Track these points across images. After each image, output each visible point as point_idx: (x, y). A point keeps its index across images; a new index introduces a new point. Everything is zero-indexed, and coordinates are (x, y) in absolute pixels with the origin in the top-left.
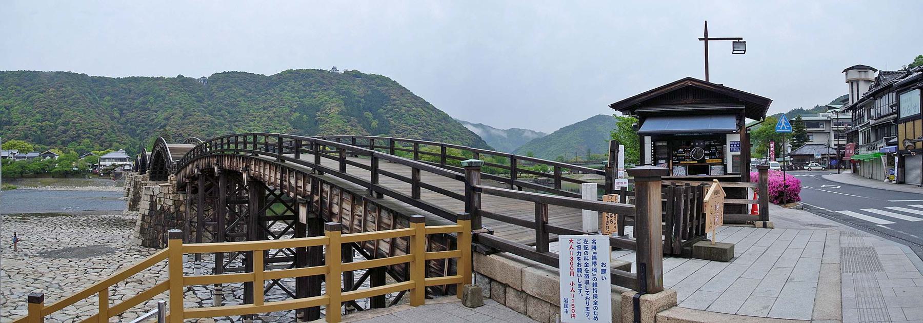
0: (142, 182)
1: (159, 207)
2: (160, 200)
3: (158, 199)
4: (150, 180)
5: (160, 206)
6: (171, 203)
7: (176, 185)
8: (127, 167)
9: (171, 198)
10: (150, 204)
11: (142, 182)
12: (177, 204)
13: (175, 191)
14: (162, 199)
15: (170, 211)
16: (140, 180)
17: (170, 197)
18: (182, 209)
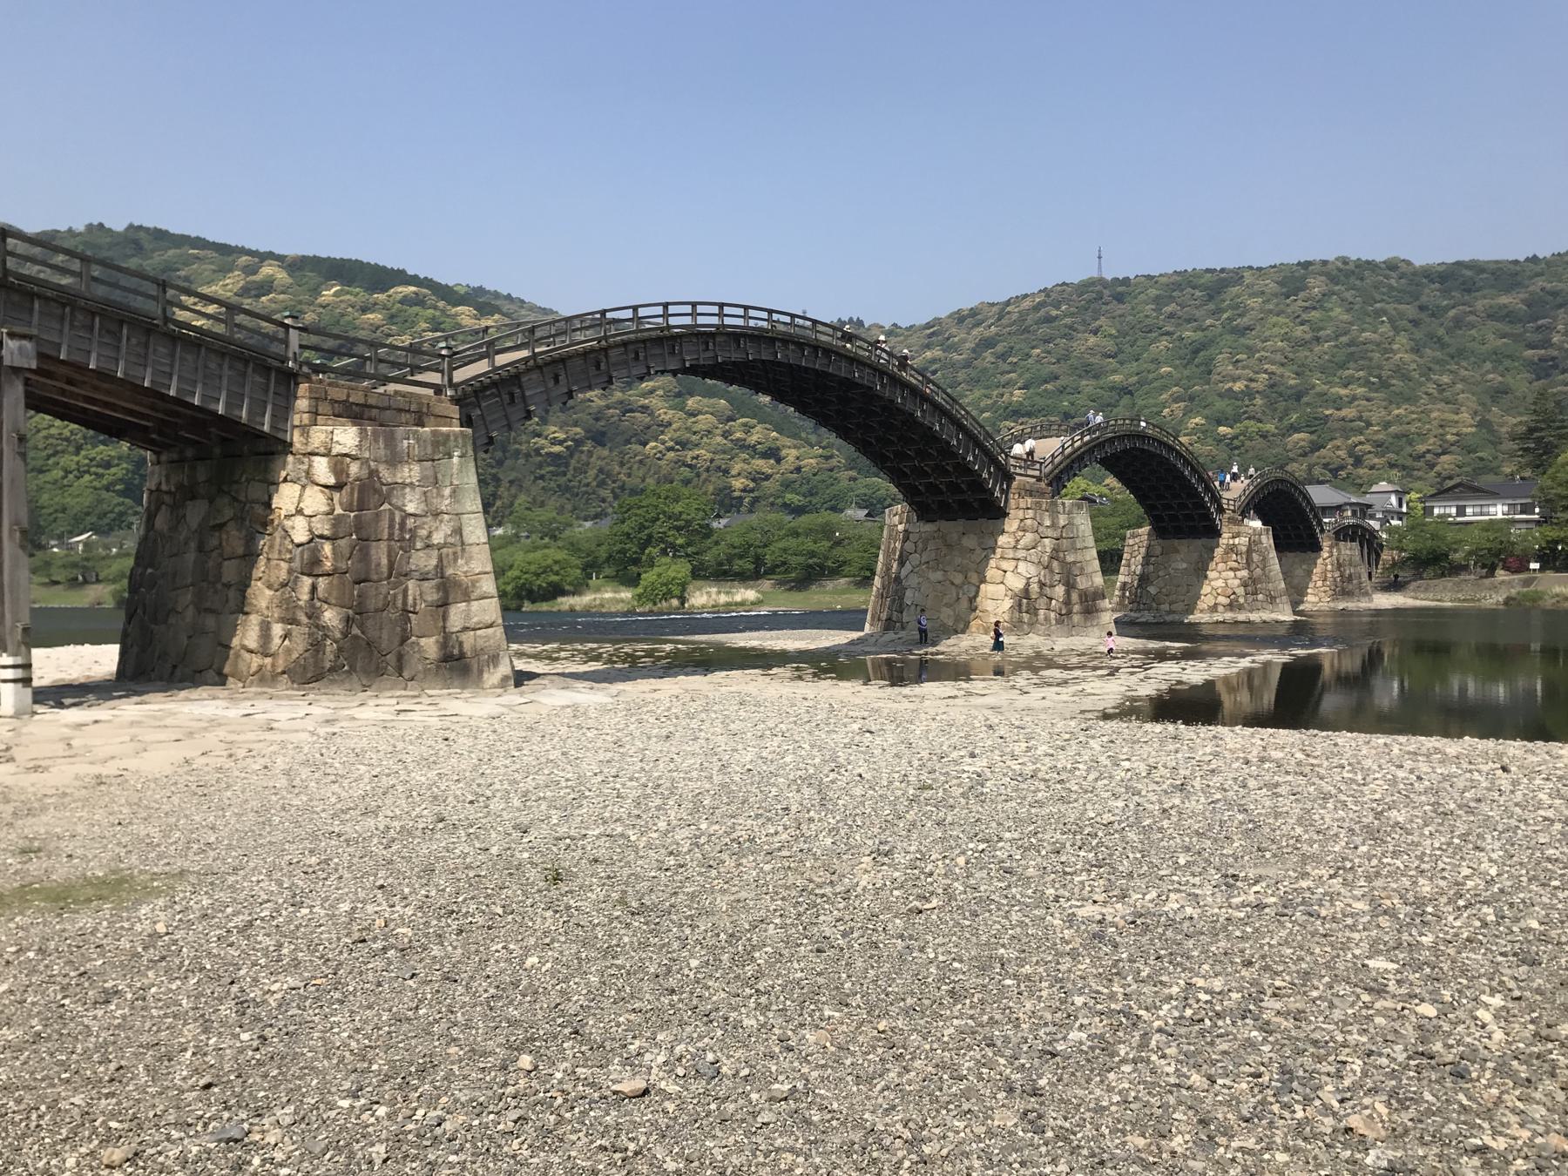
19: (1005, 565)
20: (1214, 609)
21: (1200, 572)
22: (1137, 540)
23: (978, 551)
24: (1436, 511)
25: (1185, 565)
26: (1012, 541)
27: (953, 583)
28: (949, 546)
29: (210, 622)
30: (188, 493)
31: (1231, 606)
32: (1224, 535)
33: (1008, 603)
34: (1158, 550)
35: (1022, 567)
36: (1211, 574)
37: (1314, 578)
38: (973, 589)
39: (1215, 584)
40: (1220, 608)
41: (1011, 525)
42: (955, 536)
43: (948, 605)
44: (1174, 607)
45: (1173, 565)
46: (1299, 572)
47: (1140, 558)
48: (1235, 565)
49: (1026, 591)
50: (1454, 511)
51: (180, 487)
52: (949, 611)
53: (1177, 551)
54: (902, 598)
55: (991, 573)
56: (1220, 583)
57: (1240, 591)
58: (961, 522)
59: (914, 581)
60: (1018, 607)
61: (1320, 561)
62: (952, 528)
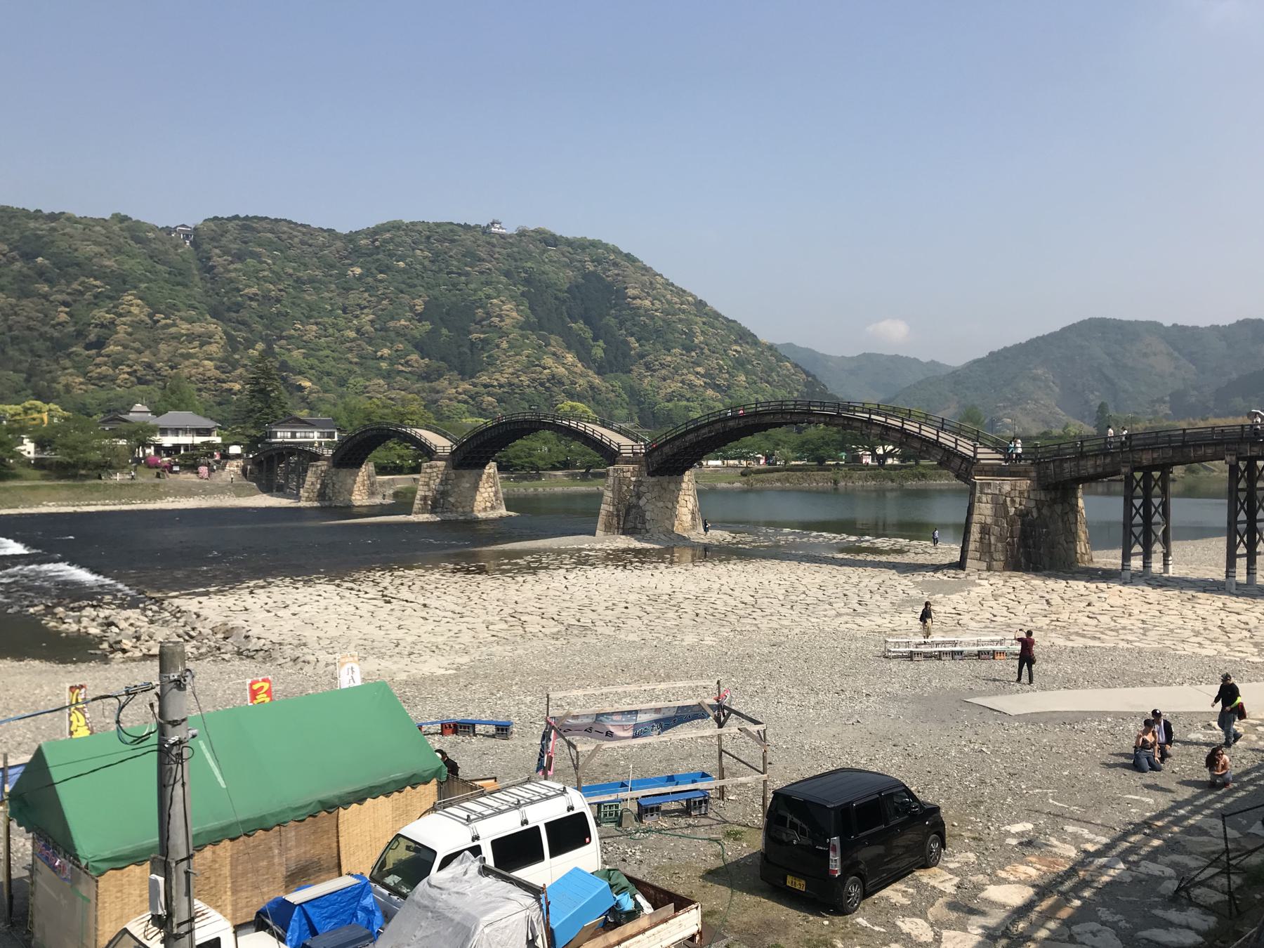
1: (1012, 511)
2: (1013, 501)
3: (1008, 499)
6: (1032, 504)
9: (1032, 497)
11: (633, 479)
12: (1039, 504)
14: (1018, 500)
16: (629, 474)
19: (687, 498)
20: (485, 509)
21: (476, 488)
24: (279, 434)
25: (468, 485)
29: (1072, 546)
30: (1054, 501)
31: (493, 508)
33: (690, 516)
36: (482, 490)
37: (358, 484)
39: (486, 495)
41: (686, 478)
46: (350, 481)
47: (438, 481)
50: (289, 434)
53: (463, 477)
54: (643, 517)
55: (682, 502)
56: (486, 495)
58: (667, 477)
59: (649, 507)
61: (360, 474)
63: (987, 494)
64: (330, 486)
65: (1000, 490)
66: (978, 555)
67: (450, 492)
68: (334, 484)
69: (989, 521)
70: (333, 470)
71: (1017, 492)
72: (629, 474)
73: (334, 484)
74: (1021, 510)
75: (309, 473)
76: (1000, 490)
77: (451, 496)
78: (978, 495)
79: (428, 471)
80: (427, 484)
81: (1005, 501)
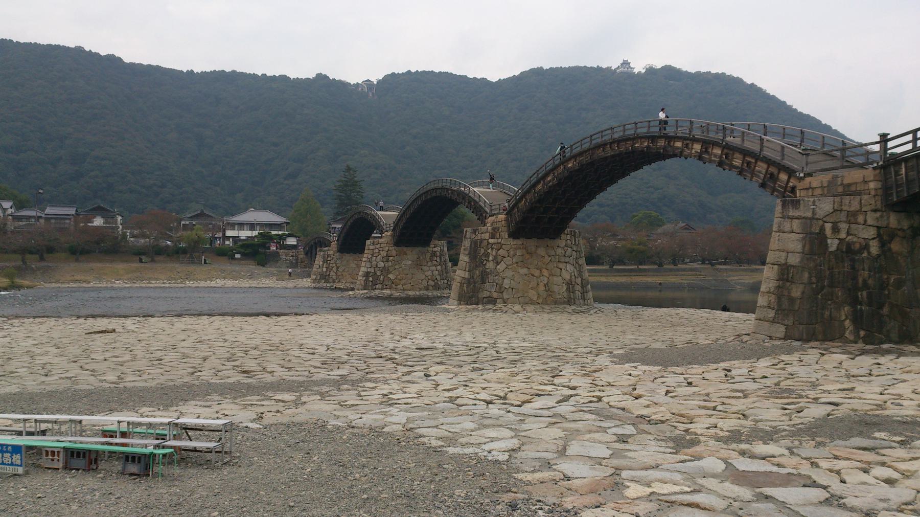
0: (491, 241)
2: (836, 230)
3: (828, 226)
4: (510, 236)
5: (837, 242)
6: (872, 232)
7: (880, 192)
8: (292, 241)
9: (870, 222)
10: (803, 239)
11: (491, 241)
12: (885, 236)
13: (879, 206)
14: (844, 226)
15: (869, 253)
16: (487, 236)
17: (865, 221)
18: (895, 246)
19: (561, 266)
22: (378, 246)
23: (547, 257)
25: (410, 263)
26: (563, 252)
27: (533, 275)
28: (530, 254)
32: (432, 246)
33: (565, 288)
34: (394, 253)
35: (569, 267)
38: (546, 279)
39: (429, 273)
40: (431, 288)
42: (533, 249)
43: (532, 289)
44: (405, 287)
45: (404, 262)
48: (435, 262)
49: (570, 280)
51: (911, 227)
52: (533, 292)
56: (429, 273)
57: (438, 278)
60: (568, 290)
62: (532, 243)
63: (792, 218)
64: (334, 269)
65: (814, 213)
66: (771, 314)
67: (391, 269)
68: (338, 268)
69: (794, 260)
70: (338, 254)
71: (844, 214)
72: (487, 236)
73: (338, 268)
74: (849, 245)
75: (318, 256)
76: (814, 213)
77: (390, 273)
78: (776, 221)
79: (371, 247)
80: (370, 262)
81: (822, 229)
